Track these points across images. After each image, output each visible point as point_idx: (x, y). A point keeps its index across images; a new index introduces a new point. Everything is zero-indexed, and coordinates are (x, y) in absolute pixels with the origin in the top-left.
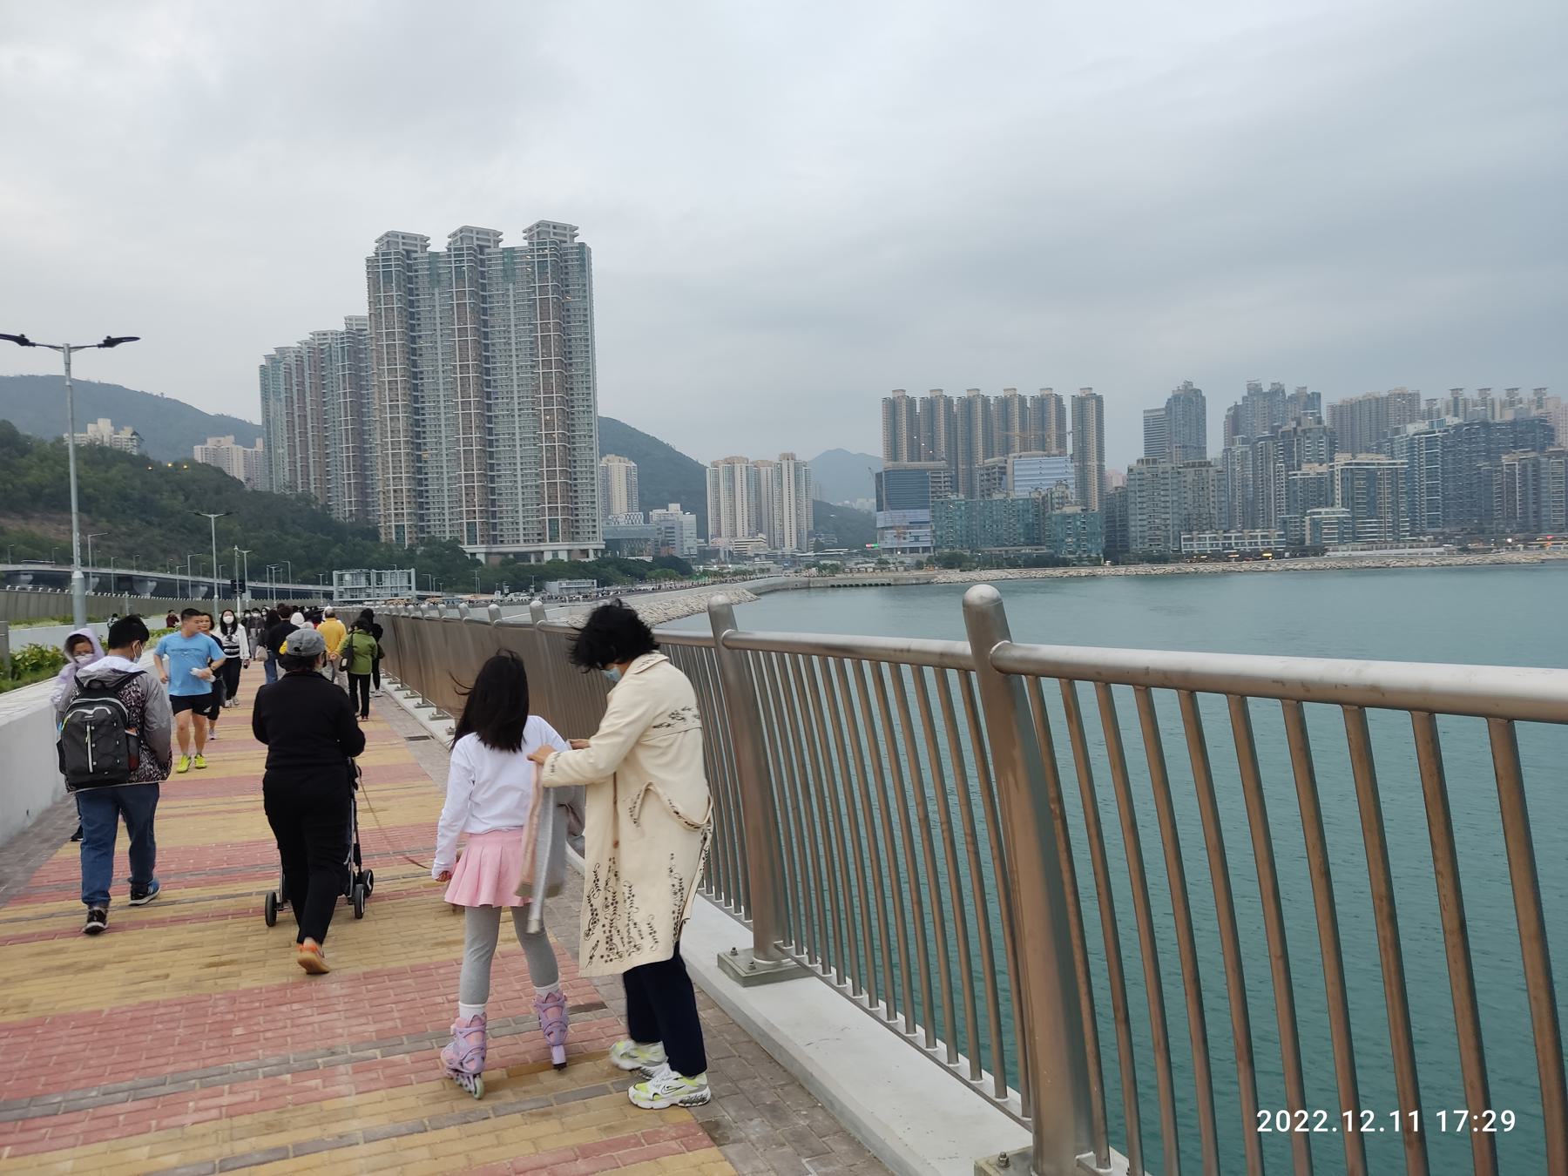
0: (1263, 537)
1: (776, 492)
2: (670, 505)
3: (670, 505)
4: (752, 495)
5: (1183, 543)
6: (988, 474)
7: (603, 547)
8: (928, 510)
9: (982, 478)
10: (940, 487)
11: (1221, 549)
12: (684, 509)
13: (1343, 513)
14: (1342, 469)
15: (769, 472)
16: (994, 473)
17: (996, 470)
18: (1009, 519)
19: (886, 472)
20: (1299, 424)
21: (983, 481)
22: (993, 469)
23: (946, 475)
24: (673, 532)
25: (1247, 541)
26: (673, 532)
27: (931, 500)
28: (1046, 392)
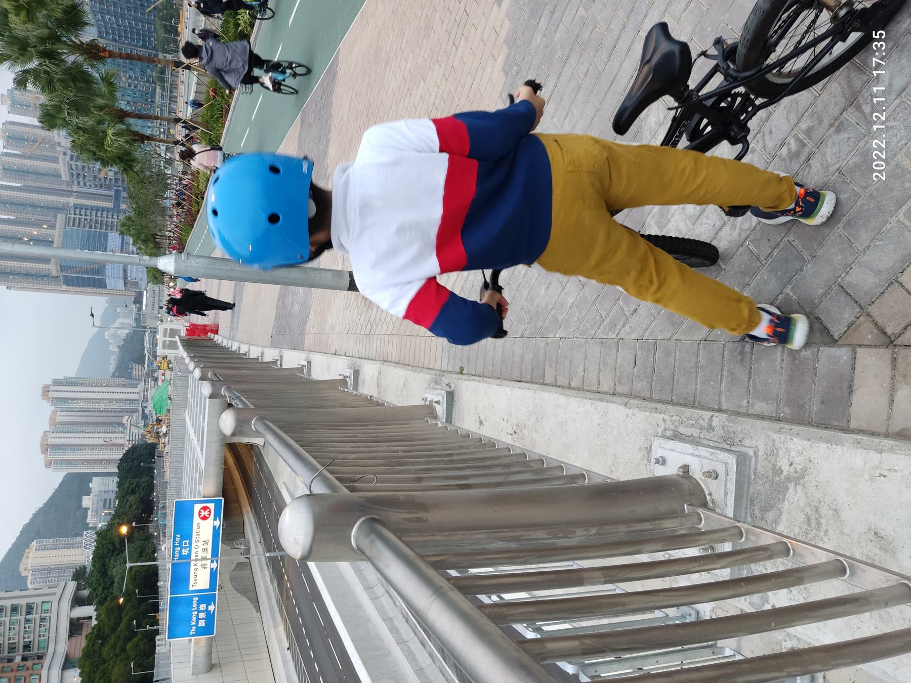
1: (82, 405)
2: (84, 506)
3: (84, 506)
4: (83, 428)
6: (78, 175)
7: (72, 585)
8: (110, 234)
9: (82, 183)
10: (85, 219)
12: (88, 492)
15: (62, 413)
16: (77, 166)
17: (73, 163)
19: (62, 271)
21: (85, 184)
22: (72, 169)
23: (73, 212)
24: (110, 500)
26: (110, 500)
27: (98, 230)
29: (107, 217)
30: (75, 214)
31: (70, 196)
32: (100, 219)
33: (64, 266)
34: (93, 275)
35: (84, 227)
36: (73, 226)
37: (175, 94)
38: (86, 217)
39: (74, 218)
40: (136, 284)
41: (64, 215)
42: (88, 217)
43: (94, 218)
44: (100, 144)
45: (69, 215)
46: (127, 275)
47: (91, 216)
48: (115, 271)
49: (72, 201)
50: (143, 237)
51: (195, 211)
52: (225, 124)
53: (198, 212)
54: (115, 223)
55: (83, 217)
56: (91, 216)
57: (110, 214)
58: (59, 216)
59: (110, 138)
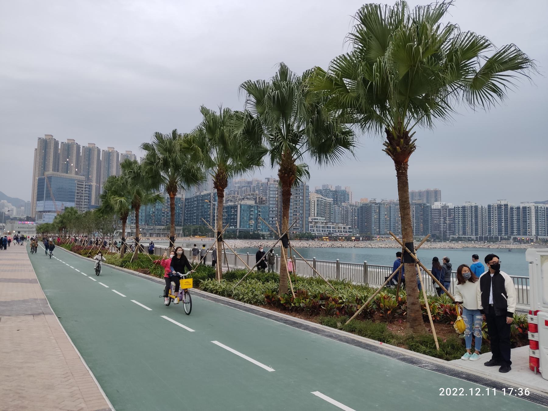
0: (344, 228)
5: (310, 229)
10: (82, 191)
11: (327, 233)
13: (323, 220)
14: (318, 200)
18: (165, 209)
19: (48, 177)
20: (269, 181)
23: (86, 184)
25: (337, 230)
27: (76, 197)
28: (130, 153)
29: (85, 202)
30: (85, 185)
31: (97, 183)
32: (84, 198)
33: (51, 179)
34: (46, 194)
35: (77, 190)
36: (78, 184)
37: (162, 236)
38: (84, 191)
39: (83, 185)
40: (40, 217)
41: (84, 180)
42: (84, 192)
43: (83, 195)
44: (116, 193)
45: (84, 182)
46: (46, 212)
47: (85, 193)
48: (49, 206)
49: (94, 184)
50: (65, 221)
51: (80, 252)
52: (137, 271)
53: (80, 254)
54: (81, 206)
55: (84, 189)
56: (85, 193)
57: (87, 203)
58: (83, 177)
59: (118, 199)
